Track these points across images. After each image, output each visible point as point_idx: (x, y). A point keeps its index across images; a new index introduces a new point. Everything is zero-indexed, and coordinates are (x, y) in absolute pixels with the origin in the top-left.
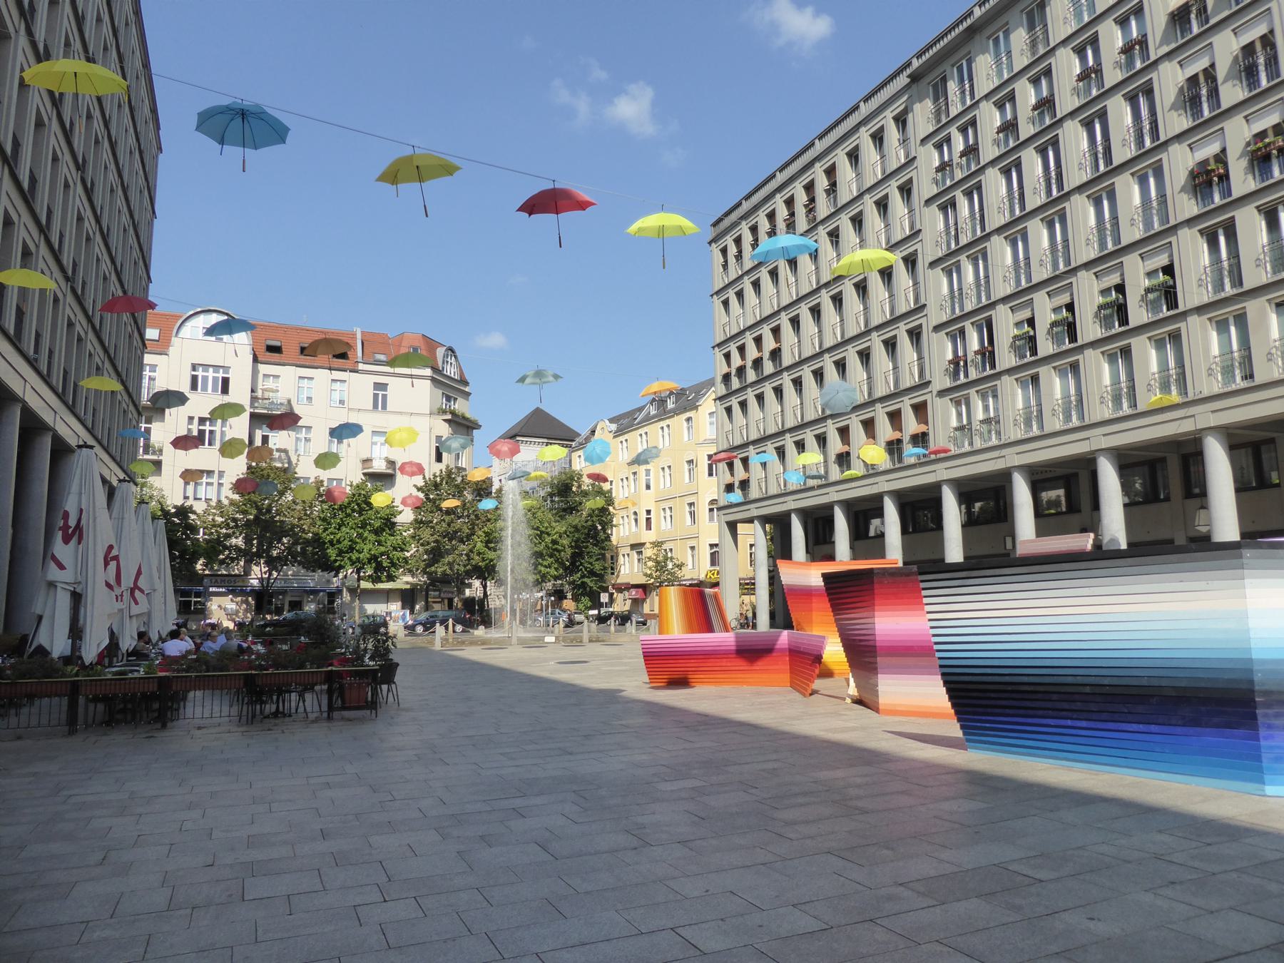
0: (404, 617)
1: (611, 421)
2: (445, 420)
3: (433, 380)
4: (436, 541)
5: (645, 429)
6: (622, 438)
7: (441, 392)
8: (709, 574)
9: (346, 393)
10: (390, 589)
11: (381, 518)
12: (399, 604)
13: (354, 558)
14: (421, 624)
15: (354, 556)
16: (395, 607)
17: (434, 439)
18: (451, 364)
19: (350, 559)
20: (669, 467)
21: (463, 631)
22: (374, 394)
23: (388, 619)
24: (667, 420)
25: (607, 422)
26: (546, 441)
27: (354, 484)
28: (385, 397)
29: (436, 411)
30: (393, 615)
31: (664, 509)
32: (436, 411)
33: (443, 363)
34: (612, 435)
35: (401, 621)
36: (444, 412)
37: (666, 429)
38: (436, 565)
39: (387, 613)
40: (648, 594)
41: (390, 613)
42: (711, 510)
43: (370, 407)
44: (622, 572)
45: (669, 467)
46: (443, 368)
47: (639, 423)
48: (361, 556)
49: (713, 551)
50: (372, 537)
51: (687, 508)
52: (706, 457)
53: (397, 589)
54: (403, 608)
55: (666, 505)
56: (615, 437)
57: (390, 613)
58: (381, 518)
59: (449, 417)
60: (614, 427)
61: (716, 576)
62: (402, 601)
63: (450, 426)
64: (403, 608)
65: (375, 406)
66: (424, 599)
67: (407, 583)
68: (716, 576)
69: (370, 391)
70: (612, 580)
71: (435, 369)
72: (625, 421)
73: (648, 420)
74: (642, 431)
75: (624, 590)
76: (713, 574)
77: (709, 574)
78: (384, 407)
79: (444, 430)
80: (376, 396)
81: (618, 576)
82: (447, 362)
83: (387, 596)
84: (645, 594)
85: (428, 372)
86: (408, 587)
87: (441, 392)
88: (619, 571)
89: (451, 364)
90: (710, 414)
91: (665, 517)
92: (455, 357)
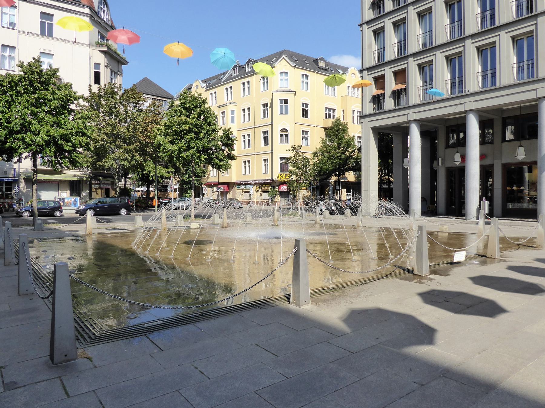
0: (75, 203)
1: (203, 81)
2: (102, 51)
3: (91, 16)
4: (102, 140)
5: (230, 85)
6: (212, 91)
7: (98, 30)
8: (280, 177)
9: (16, 17)
10: (60, 180)
11: (58, 99)
12: (68, 192)
13: (28, 140)
14: (91, 208)
15: (29, 137)
16: (65, 194)
17: (93, 66)
18: (104, 11)
19: (23, 140)
20: (249, 109)
21: (127, 214)
22: (41, 22)
23: (62, 204)
24: (248, 78)
25: (201, 82)
26: (152, 97)
27: (25, 64)
28: (51, 26)
29: (94, 44)
30: (66, 201)
31: (244, 136)
32: (94, 43)
33: (98, 8)
34: (204, 89)
35: (73, 206)
36: (101, 45)
37: (246, 84)
38: (104, 160)
39: (60, 199)
40: (230, 188)
41: (63, 199)
42: (281, 135)
43: (38, 32)
44: (211, 175)
45: (249, 109)
46: (99, 12)
47: (225, 81)
48: (38, 138)
49: (282, 162)
50: (49, 118)
51: (262, 135)
52: (279, 101)
53: (66, 181)
54: (72, 195)
55: (246, 133)
56: (206, 91)
57: (63, 199)
58: (58, 99)
59: (105, 49)
60: (204, 85)
61: (284, 177)
62: (70, 190)
63: (106, 57)
64: (72, 195)
65: (42, 33)
66: (88, 188)
67: (75, 176)
68: (284, 177)
69: (37, 19)
70: (204, 180)
71: (91, 9)
72: (213, 82)
73: (231, 79)
74: (228, 86)
75: (212, 186)
76: (282, 177)
77: (280, 177)
78: (51, 35)
79: (102, 59)
80: (42, 24)
81: (208, 178)
82: (101, 8)
83: (58, 185)
84: (229, 189)
85: (87, 11)
86: (76, 179)
87: (98, 30)
88: (209, 175)
89: (104, 11)
90: (281, 73)
91: (244, 141)
92: (107, 7)
